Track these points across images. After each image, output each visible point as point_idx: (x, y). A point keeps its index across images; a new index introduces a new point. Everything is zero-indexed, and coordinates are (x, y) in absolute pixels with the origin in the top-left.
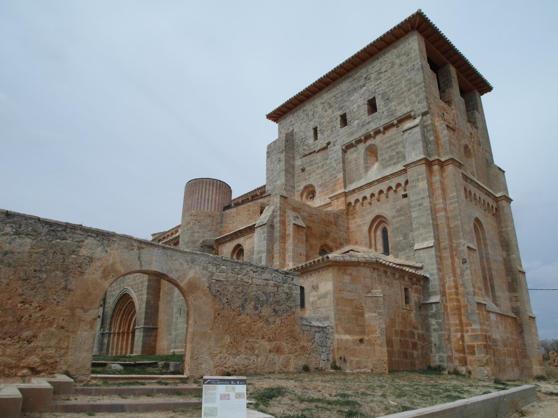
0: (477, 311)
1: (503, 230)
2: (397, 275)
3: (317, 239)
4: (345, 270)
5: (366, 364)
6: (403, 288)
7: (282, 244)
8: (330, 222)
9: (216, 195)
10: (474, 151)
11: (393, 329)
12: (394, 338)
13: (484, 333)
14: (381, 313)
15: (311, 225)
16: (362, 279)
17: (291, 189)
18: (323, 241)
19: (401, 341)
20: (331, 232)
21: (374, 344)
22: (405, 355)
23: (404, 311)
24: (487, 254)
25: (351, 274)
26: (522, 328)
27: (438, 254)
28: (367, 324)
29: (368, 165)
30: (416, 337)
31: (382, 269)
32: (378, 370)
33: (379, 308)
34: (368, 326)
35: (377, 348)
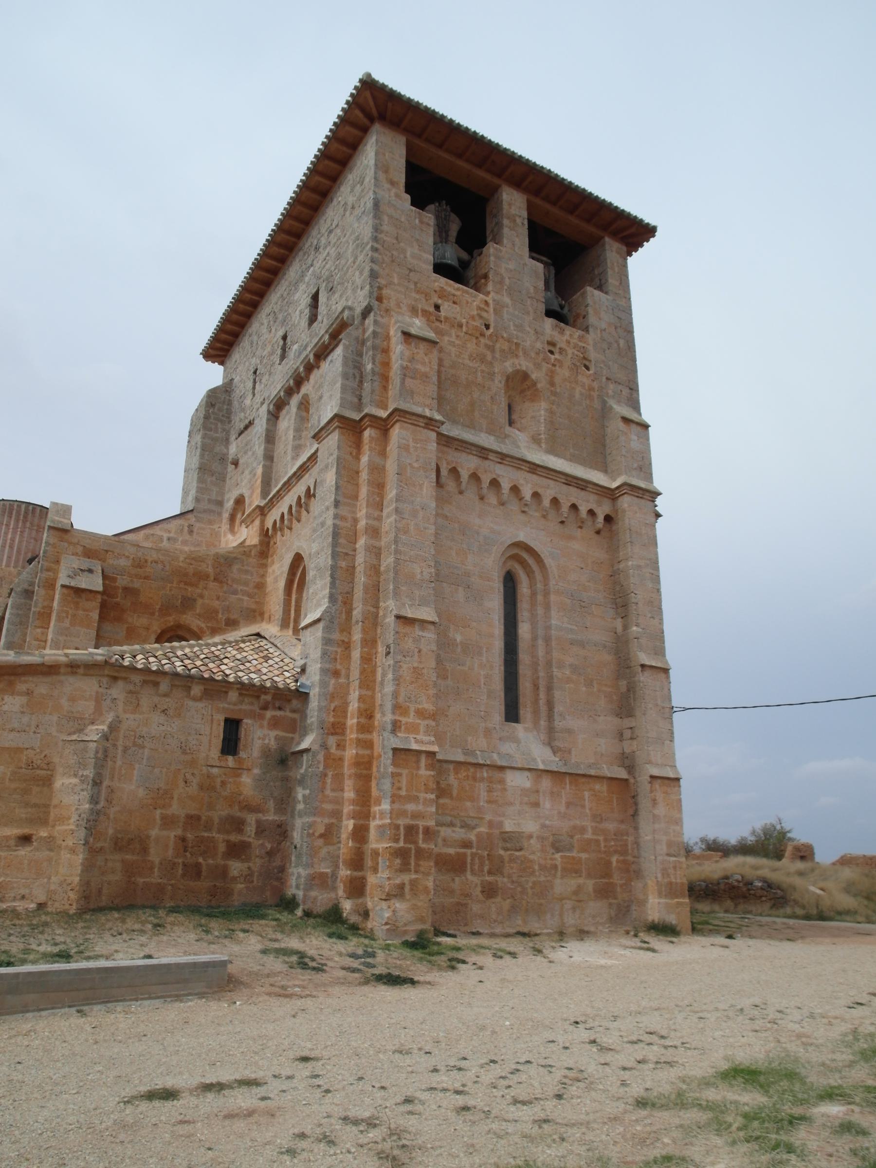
0: (391, 769)
1: (621, 566)
2: (197, 690)
3: (153, 614)
4: (11, 684)
5: (23, 891)
6: (221, 718)
7: (39, 630)
8: (202, 576)
9: (14, 533)
10: (552, 384)
11: (158, 812)
12: (154, 833)
13: (402, 822)
14: (87, 776)
15: (137, 584)
16: (64, 702)
17: (213, 507)
18: (171, 618)
19: (184, 839)
20: (201, 596)
21: (60, 847)
22: (194, 871)
23: (215, 771)
24: (548, 628)
25: (29, 693)
26: (636, 804)
27: (336, 636)
28: (55, 802)
29: (302, 442)
30: (251, 829)
31: (137, 678)
32: (57, 905)
33: (85, 767)
34: (55, 806)
35: (65, 855)
